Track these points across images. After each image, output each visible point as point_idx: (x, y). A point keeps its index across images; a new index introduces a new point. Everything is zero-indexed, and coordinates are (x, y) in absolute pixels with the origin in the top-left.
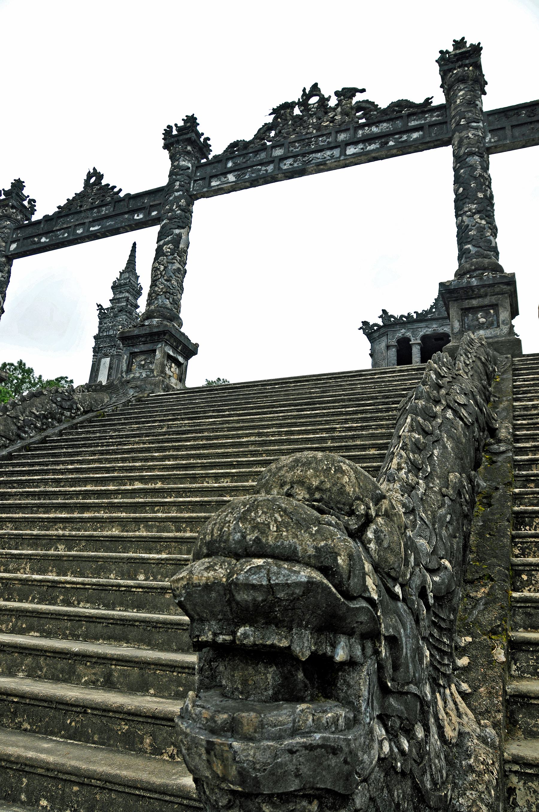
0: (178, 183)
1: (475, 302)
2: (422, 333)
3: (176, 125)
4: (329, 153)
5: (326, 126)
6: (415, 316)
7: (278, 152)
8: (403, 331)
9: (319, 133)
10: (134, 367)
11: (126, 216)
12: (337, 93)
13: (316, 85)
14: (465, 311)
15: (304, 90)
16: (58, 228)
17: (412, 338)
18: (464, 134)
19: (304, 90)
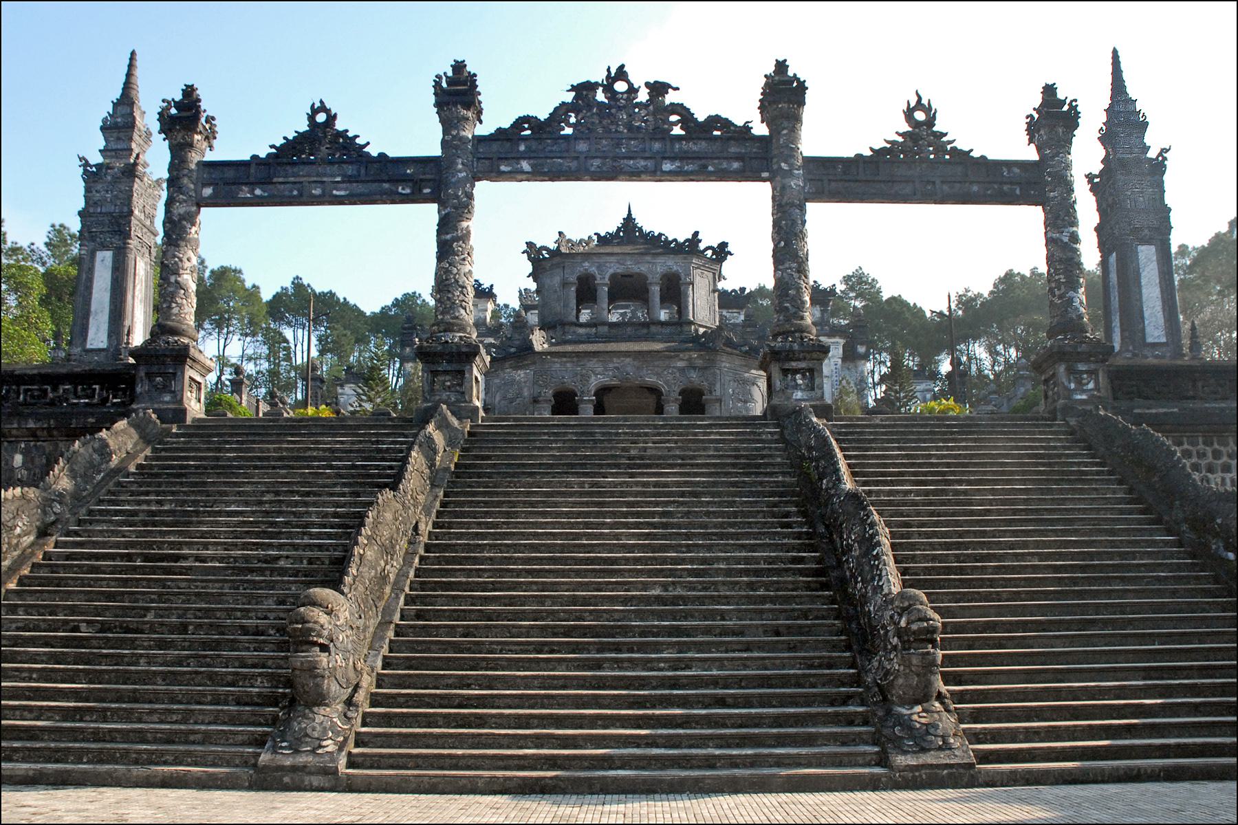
1: (794, 364)
2: (611, 271)
4: (643, 163)
7: (582, 146)
8: (586, 264)
9: (632, 136)
11: (386, 185)
12: (647, 85)
13: (622, 66)
14: (785, 372)
15: (609, 70)
16: (281, 180)
17: (598, 277)
18: (786, 181)
19: (609, 70)
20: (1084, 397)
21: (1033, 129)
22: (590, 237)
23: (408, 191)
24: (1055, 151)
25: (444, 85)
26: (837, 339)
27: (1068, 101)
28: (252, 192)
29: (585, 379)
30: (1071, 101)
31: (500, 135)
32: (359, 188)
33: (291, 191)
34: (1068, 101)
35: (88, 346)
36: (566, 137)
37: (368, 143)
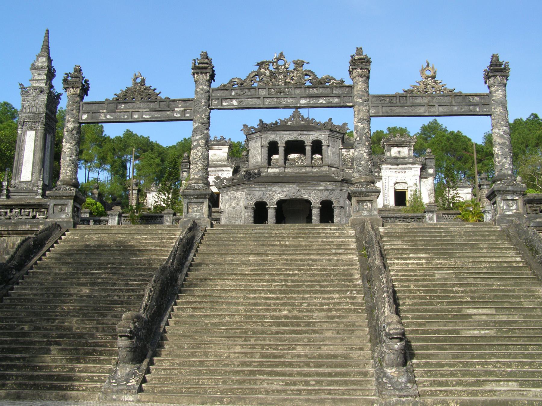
0: (203, 101)
2: (286, 139)
3: (197, 59)
5: (289, 83)
6: (279, 121)
8: (273, 136)
9: (286, 87)
10: (190, 210)
20: (510, 213)
21: (487, 77)
22: (276, 121)
23: (179, 115)
24: (497, 89)
25: (197, 64)
26: (417, 166)
27: (504, 63)
28: (105, 116)
29: (272, 196)
30: (506, 63)
31: (224, 88)
32: (157, 115)
33: (124, 116)
34: (504, 63)
35: (22, 180)
36: (254, 88)
37: (160, 93)
